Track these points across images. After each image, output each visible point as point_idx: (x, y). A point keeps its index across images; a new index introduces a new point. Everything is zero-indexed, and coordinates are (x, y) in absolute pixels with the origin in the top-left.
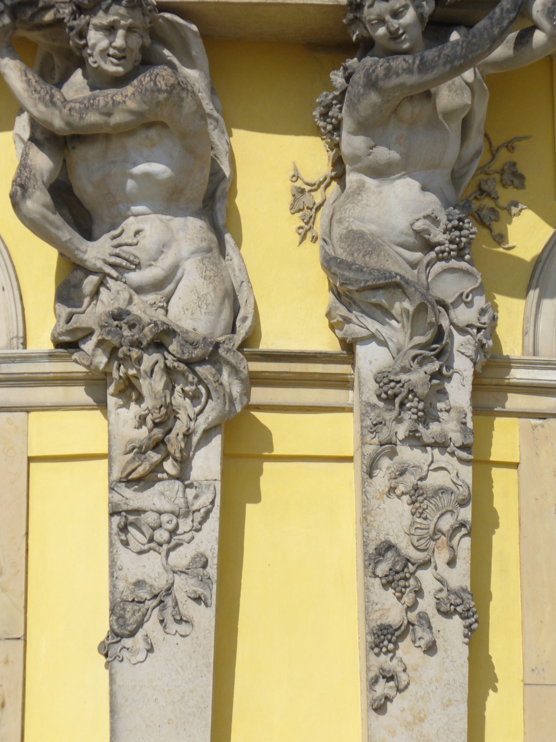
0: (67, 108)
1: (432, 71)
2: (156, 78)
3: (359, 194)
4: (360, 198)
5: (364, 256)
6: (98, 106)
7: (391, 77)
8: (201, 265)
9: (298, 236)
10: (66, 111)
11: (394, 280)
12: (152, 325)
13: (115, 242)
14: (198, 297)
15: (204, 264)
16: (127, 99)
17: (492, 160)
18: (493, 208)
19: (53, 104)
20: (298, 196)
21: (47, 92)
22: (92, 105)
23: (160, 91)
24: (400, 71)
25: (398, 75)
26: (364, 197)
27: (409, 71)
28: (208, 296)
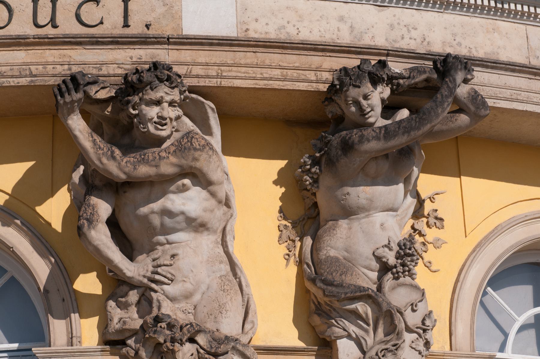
0: (124, 161)
1: (394, 139)
2: (192, 140)
3: (334, 229)
4: (335, 232)
5: (341, 275)
6: (148, 160)
7: (364, 142)
8: (220, 281)
9: (286, 261)
10: (123, 163)
11: (367, 293)
12: (189, 326)
13: (155, 263)
14: (219, 305)
15: (222, 280)
16: (170, 155)
17: (420, 208)
18: (423, 242)
19: (113, 158)
20: (284, 231)
21: (109, 149)
22: (144, 158)
23: (195, 149)
24: (371, 138)
25: (369, 141)
26: (338, 231)
27: (377, 138)
28: (227, 305)
